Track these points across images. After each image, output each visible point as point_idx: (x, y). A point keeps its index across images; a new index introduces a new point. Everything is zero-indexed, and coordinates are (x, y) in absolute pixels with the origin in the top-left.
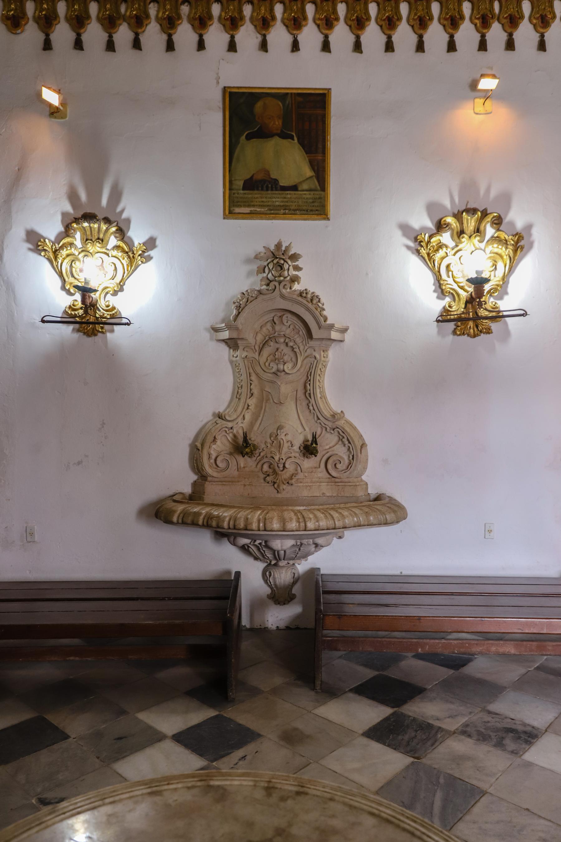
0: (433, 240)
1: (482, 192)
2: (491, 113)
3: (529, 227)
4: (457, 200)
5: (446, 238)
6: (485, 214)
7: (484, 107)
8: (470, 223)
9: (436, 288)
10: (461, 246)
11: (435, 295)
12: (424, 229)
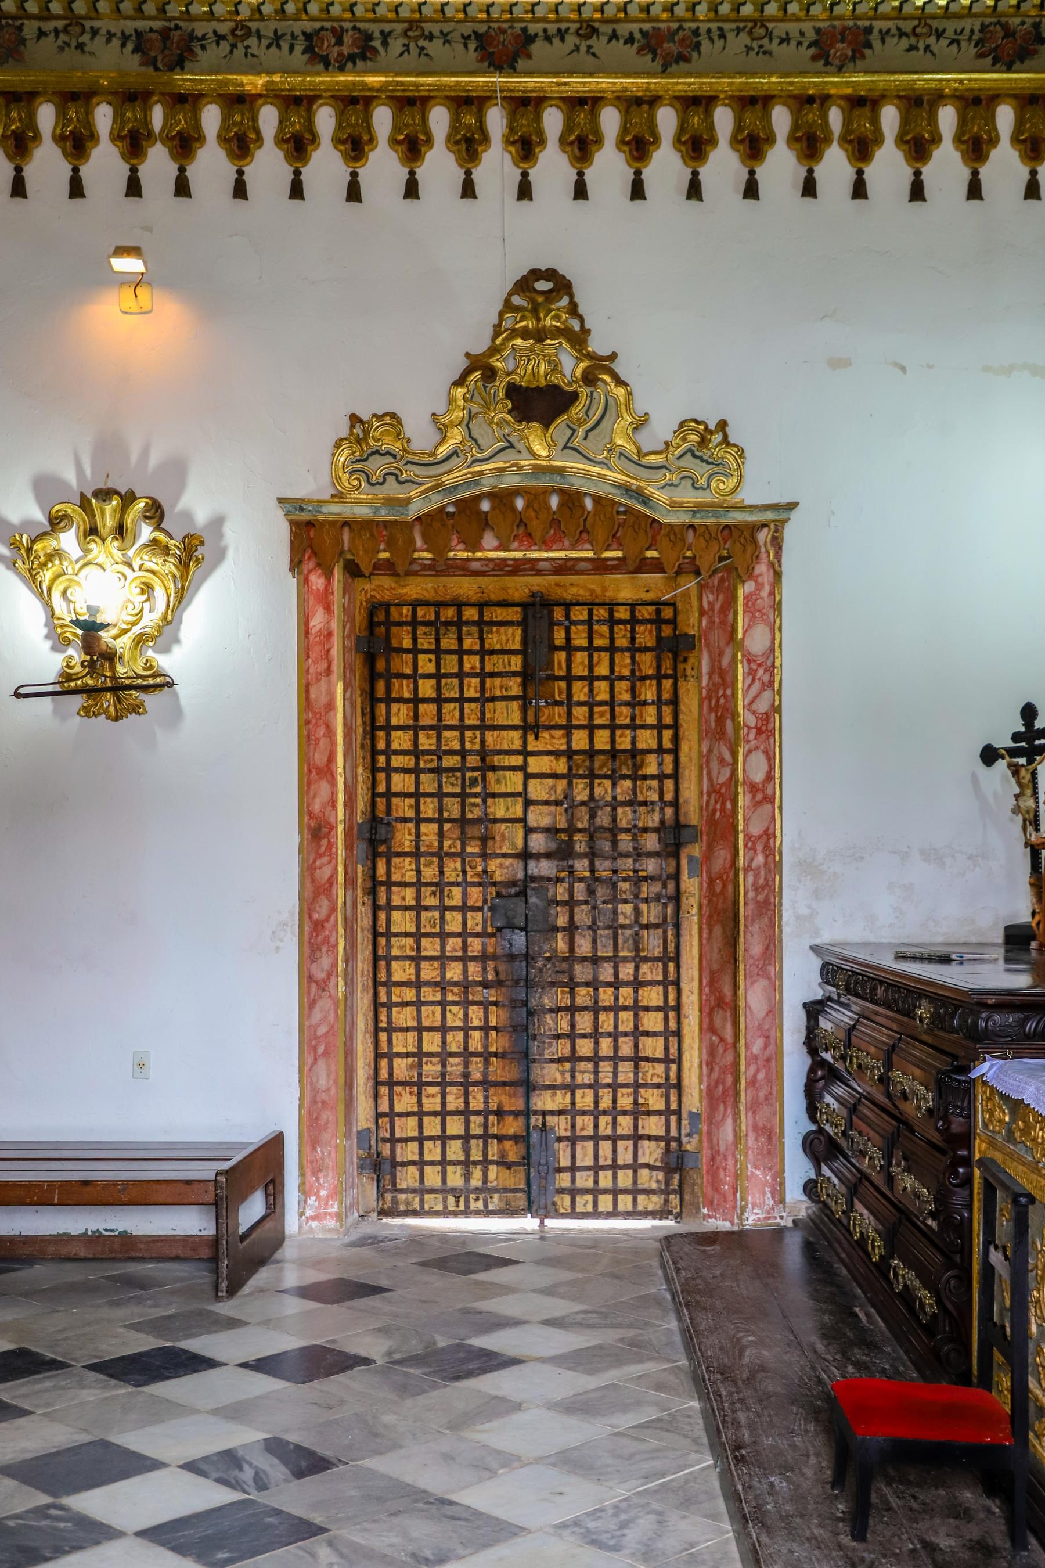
0: (38, 546)
1: (134, 457)
2: (150, 312)
3: (217, 523)
4: (88, 471)
5: (68, 540)
6: (128, 499)
7: (137, 301)
8: (108, 514)
9: (49, 631)
10: (90, 556)
11: (48, 644)
12: (27, 524)
